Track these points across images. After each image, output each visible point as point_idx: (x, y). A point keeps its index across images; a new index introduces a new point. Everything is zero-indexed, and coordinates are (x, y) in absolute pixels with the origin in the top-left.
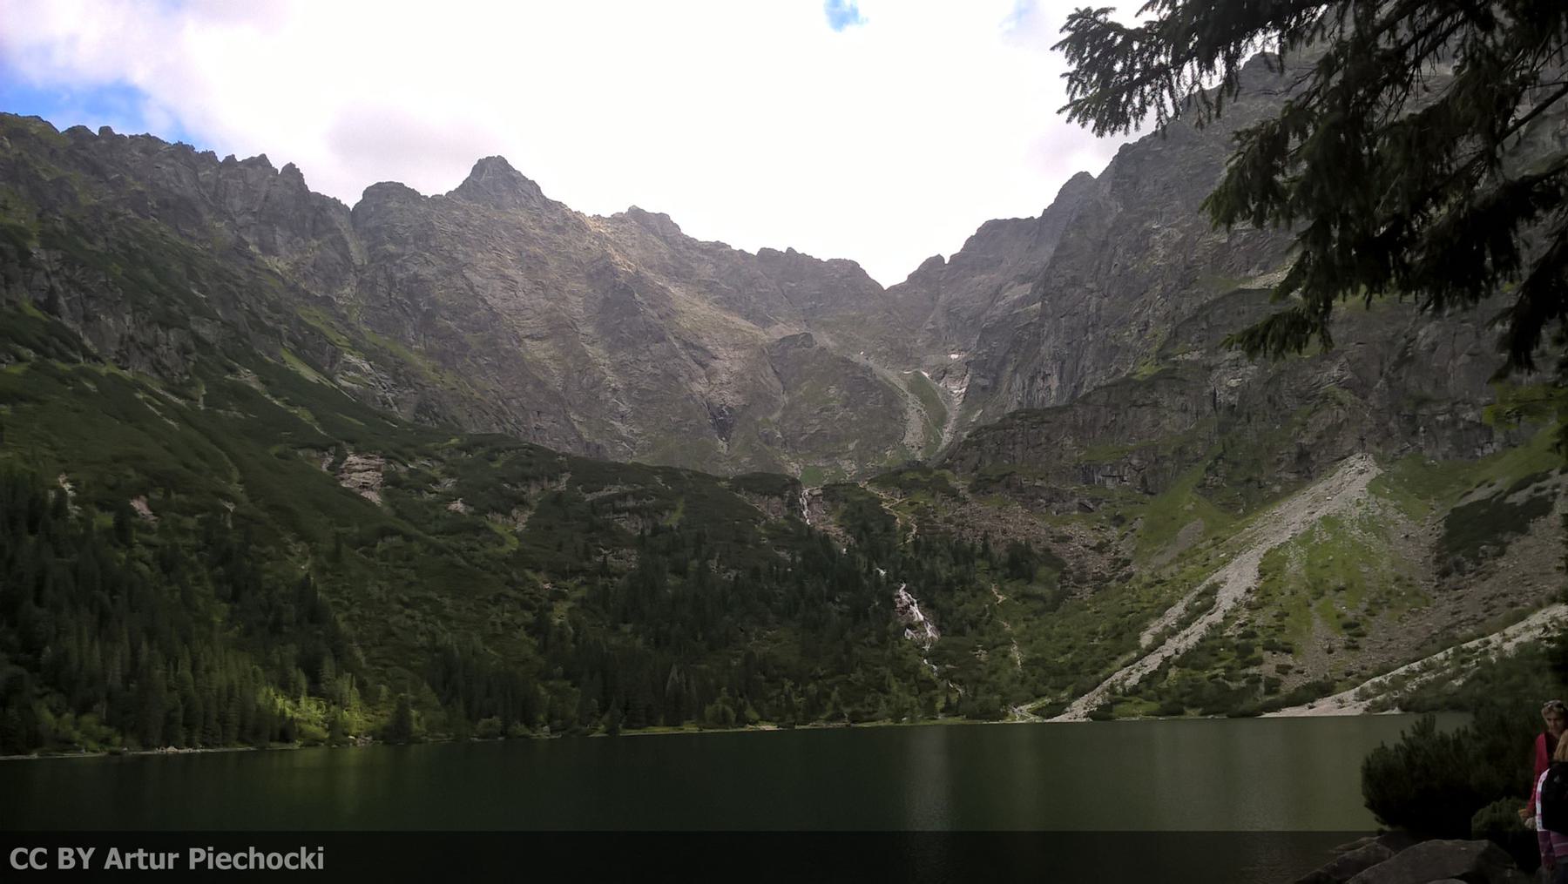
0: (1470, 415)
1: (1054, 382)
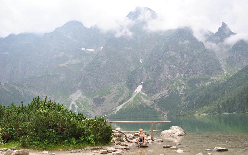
0: (91, 87)
1: (20, 70)
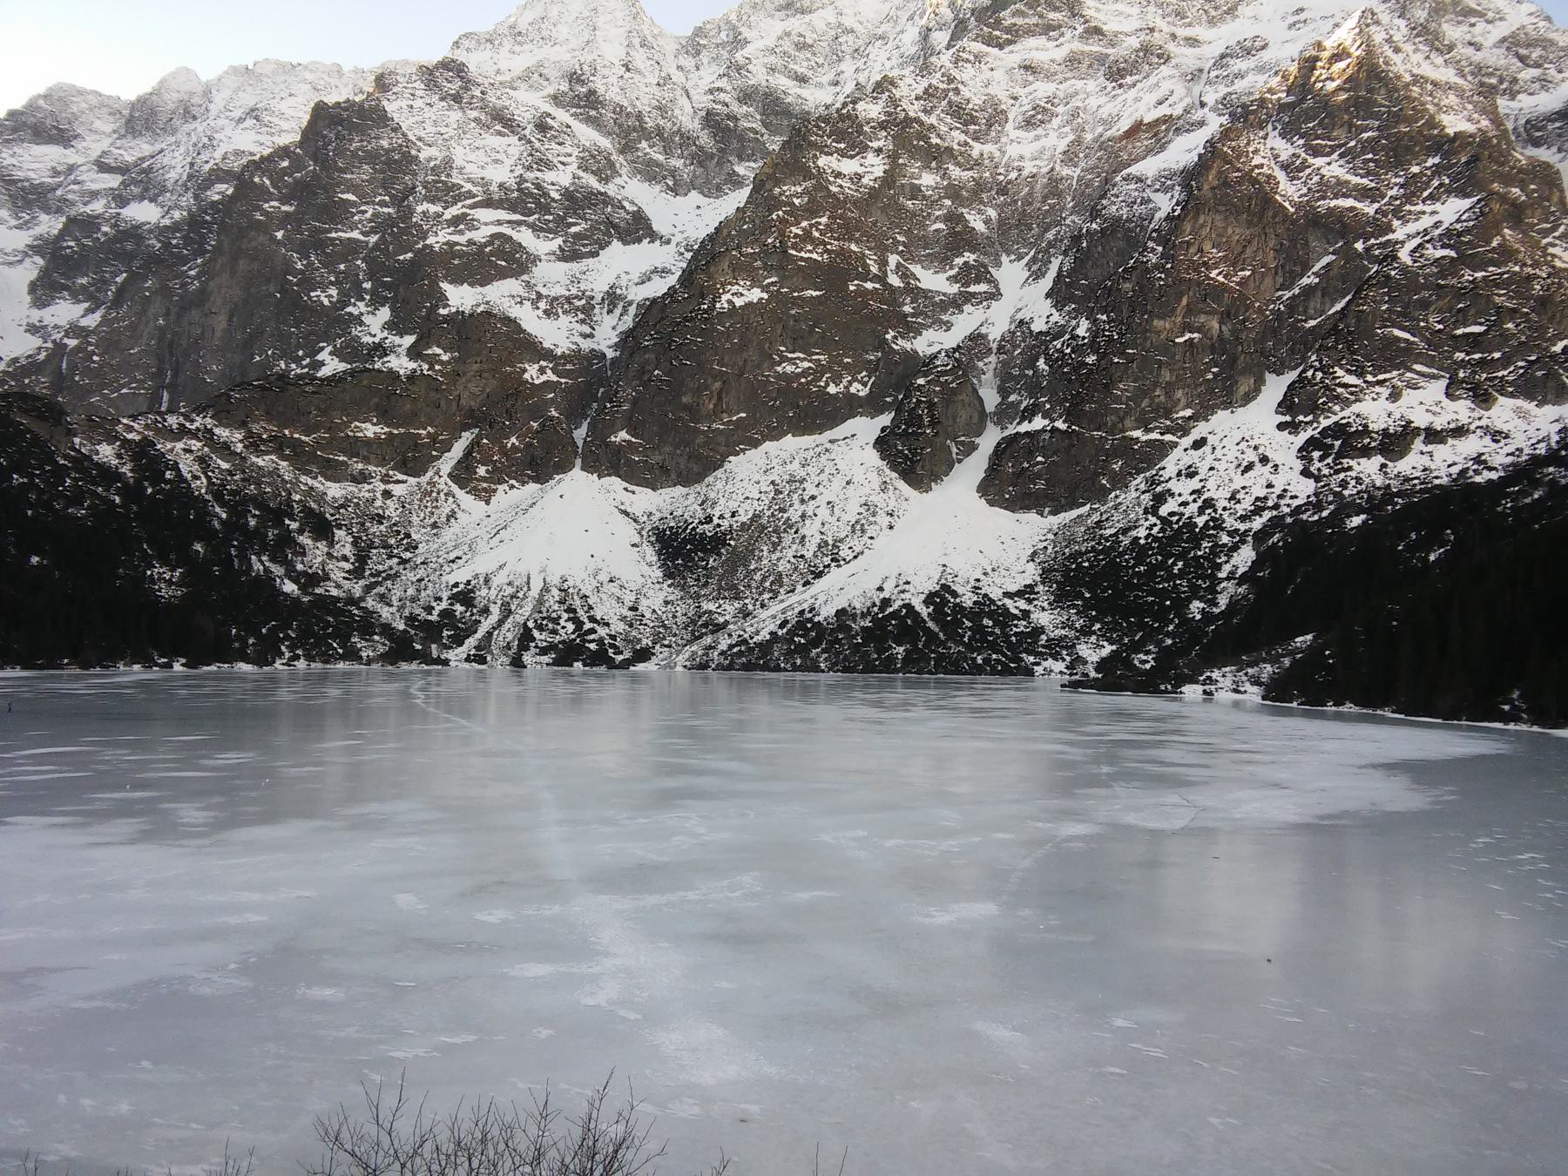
1: (220, 323)
